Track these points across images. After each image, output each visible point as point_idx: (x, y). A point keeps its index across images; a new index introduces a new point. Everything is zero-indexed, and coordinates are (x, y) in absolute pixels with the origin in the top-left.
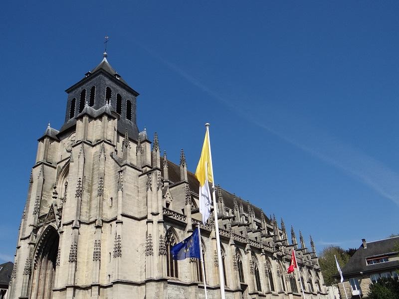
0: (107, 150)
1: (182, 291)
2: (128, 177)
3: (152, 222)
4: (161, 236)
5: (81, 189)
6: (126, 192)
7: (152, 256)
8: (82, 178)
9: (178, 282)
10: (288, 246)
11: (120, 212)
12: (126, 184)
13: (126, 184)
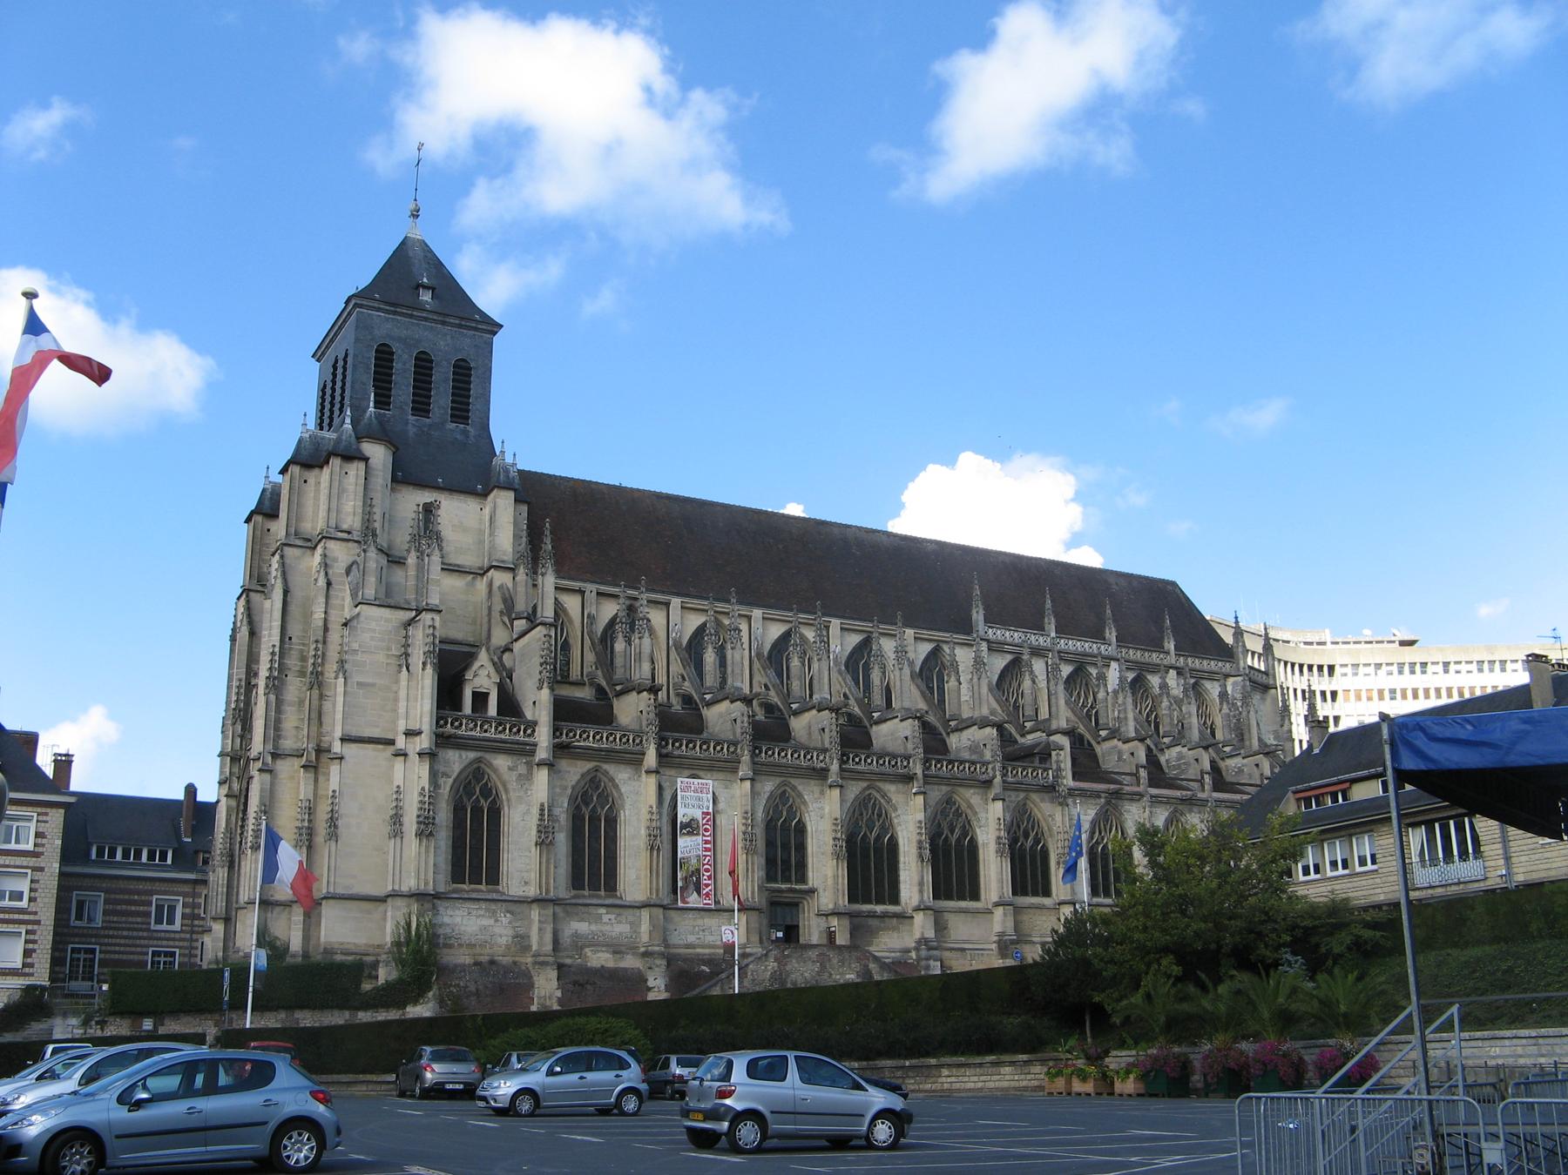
0: (335, 560)
1: (505, 919)
2: (366, 636)
3: (405, 755)
4: (423, 789)
5: (276, 674)
6: (356, 678)
7: (398, 839)
8: (278, 644)
9: (494, 896)
10: (1126, 741)
11: (338, 734)
12: (359, 657)
13: (359, 657)
